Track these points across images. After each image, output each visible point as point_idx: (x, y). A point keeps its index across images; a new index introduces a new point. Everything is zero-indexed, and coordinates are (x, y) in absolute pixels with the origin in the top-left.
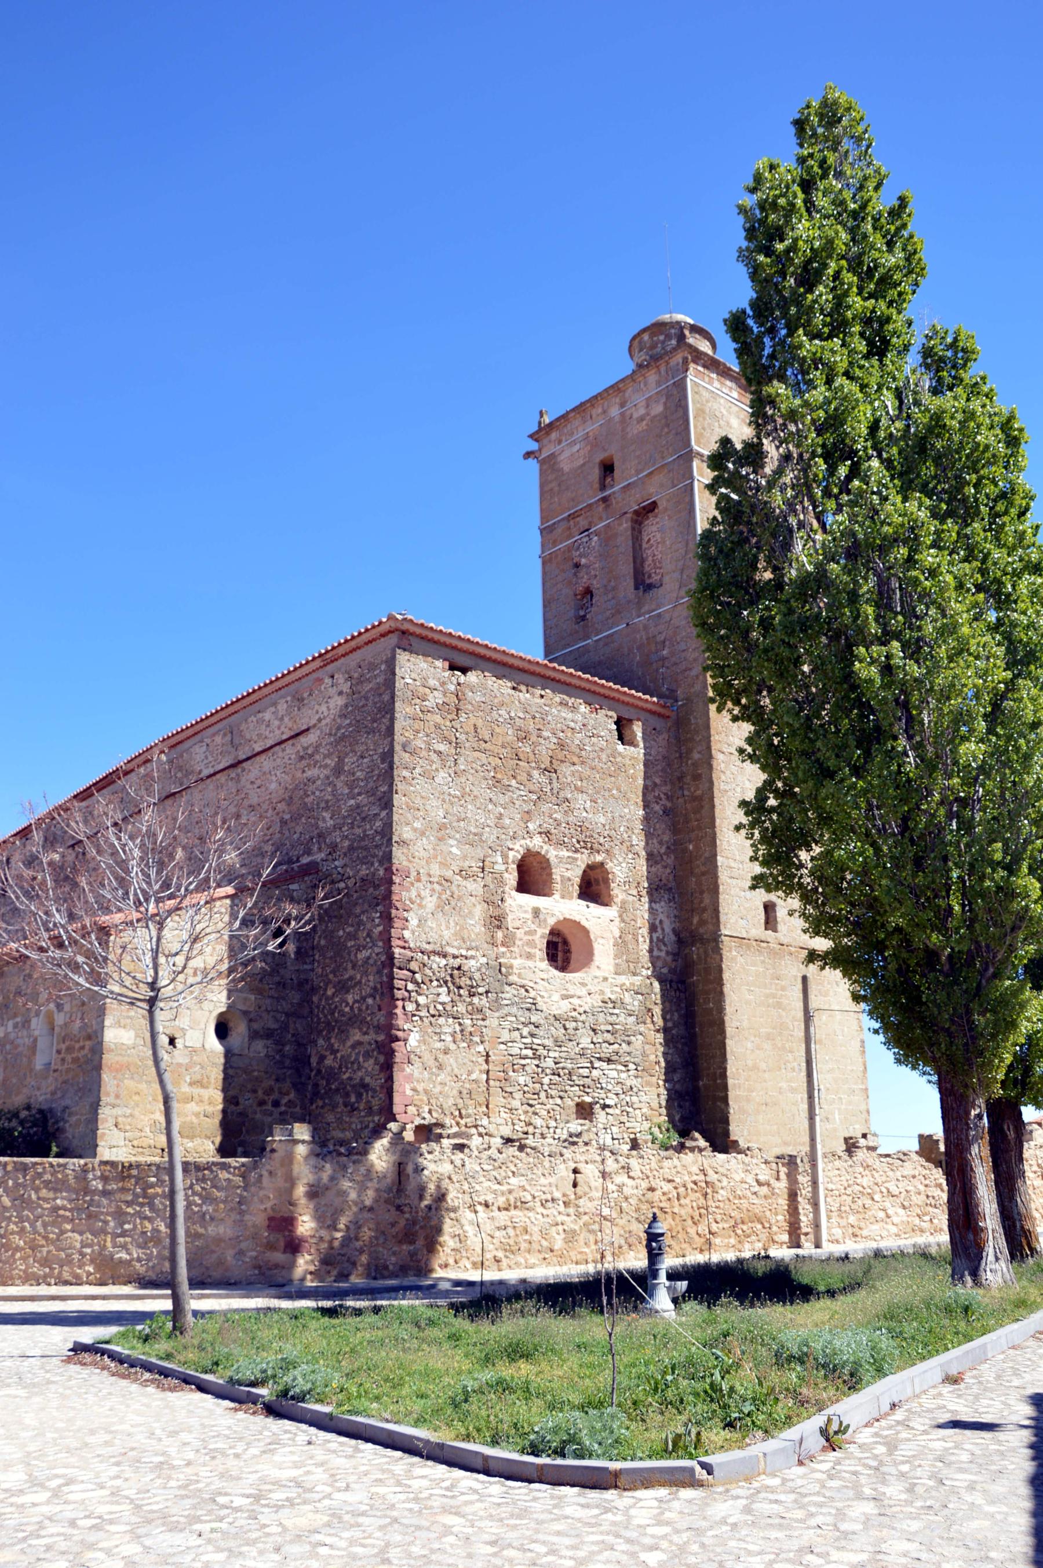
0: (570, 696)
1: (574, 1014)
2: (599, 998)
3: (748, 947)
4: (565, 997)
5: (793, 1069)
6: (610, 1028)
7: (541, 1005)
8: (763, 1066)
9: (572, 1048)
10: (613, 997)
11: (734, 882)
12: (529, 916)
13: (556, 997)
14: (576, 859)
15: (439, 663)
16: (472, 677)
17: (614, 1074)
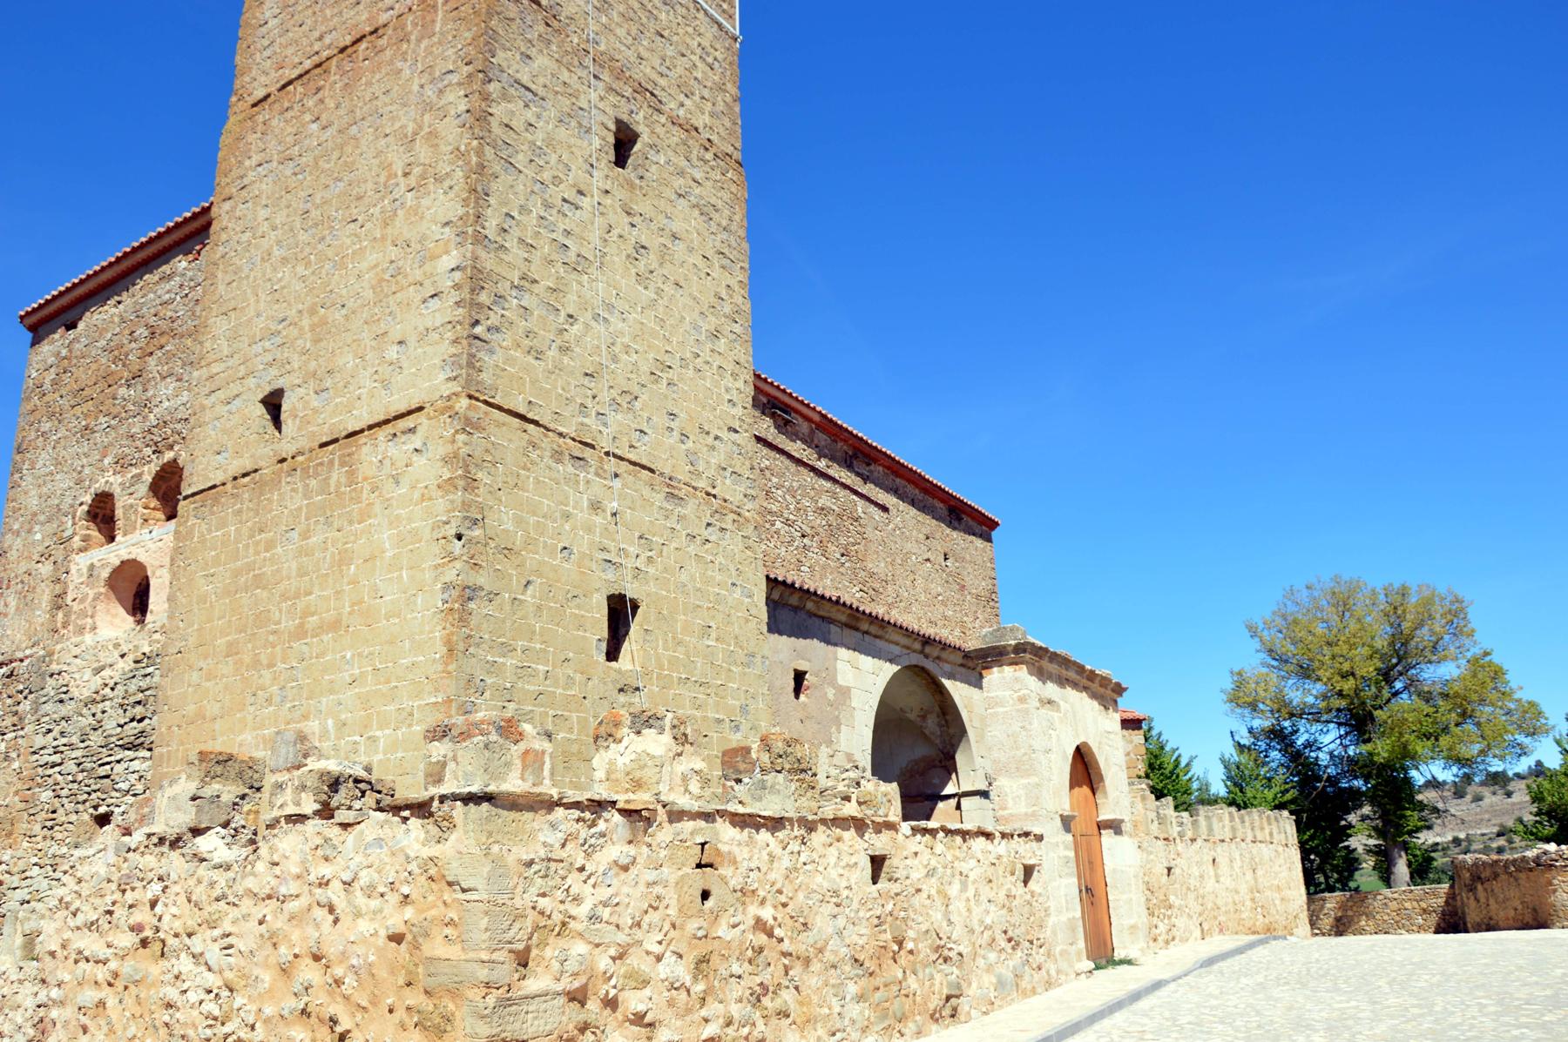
0: (167, 262)
1: (107, 690)
2: (130, 658)
3: (216, 501)
4: (98, 671)
5: (269, 701)
6: (140, 696)
7: (75, 692)
8: (213, 709)
9: (96, 739)
10: (147, 649)
11: (213, 398)
12: (84, 579)
13: (88, 674)
14: (140, 475)
15: (56, 336)
16: (81, 325)
17: (136, 765)
